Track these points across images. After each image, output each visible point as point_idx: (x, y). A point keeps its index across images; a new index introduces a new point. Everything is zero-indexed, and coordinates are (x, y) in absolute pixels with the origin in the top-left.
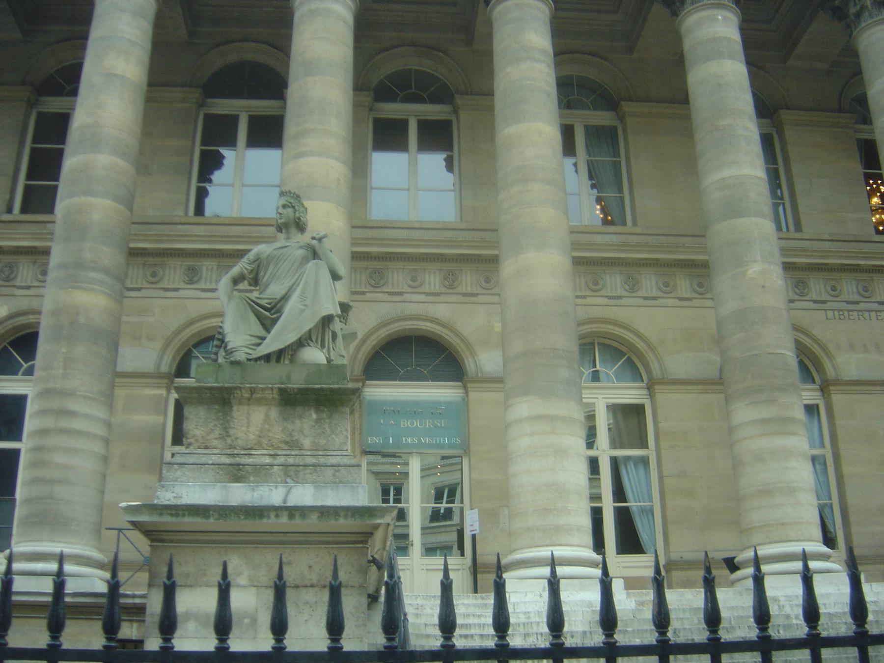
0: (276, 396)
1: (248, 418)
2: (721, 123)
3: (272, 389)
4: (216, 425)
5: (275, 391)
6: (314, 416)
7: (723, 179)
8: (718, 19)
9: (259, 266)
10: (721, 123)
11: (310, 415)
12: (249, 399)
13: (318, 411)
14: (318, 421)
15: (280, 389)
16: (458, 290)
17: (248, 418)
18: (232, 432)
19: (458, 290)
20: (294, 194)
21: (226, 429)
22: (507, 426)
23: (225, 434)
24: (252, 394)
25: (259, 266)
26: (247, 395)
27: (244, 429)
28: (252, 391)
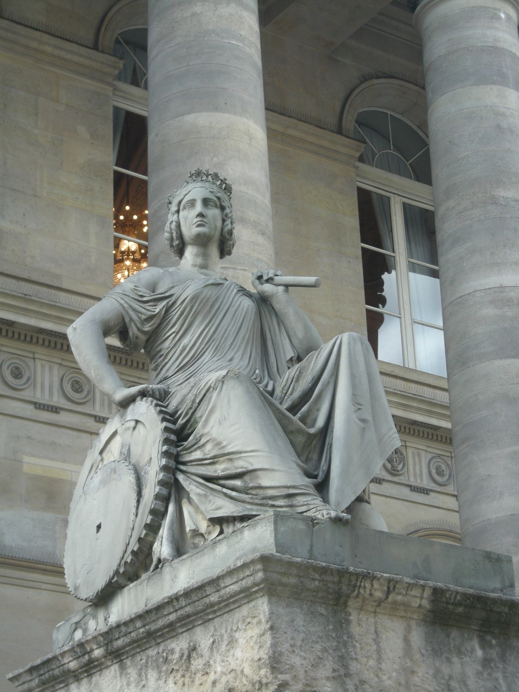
0: (425, 603)
1: (377, 641)
2: (502, 193)
3: (423, 587)
4: (325, 650)
5: (427, 593)
6: (479, 653)
7: (502, 288)
8: (500, 18)
9: (168, 309)
10: (502, 193)
11: (473, 650)
12: (379, 603)
13: (484, 644)
14: (486, 662)
15: (436, 591)
16: (27, 394)
17: (377, 641)
18: (354, 666)
19: (27, 394)
20: (223, 181)
21: (343, 660)
22: (304, 691)
23: (342, 672)
24: (388, 592)
25: (168, 309)
26: (378, 594)
27: (372, 663)
28: (391, 586)
